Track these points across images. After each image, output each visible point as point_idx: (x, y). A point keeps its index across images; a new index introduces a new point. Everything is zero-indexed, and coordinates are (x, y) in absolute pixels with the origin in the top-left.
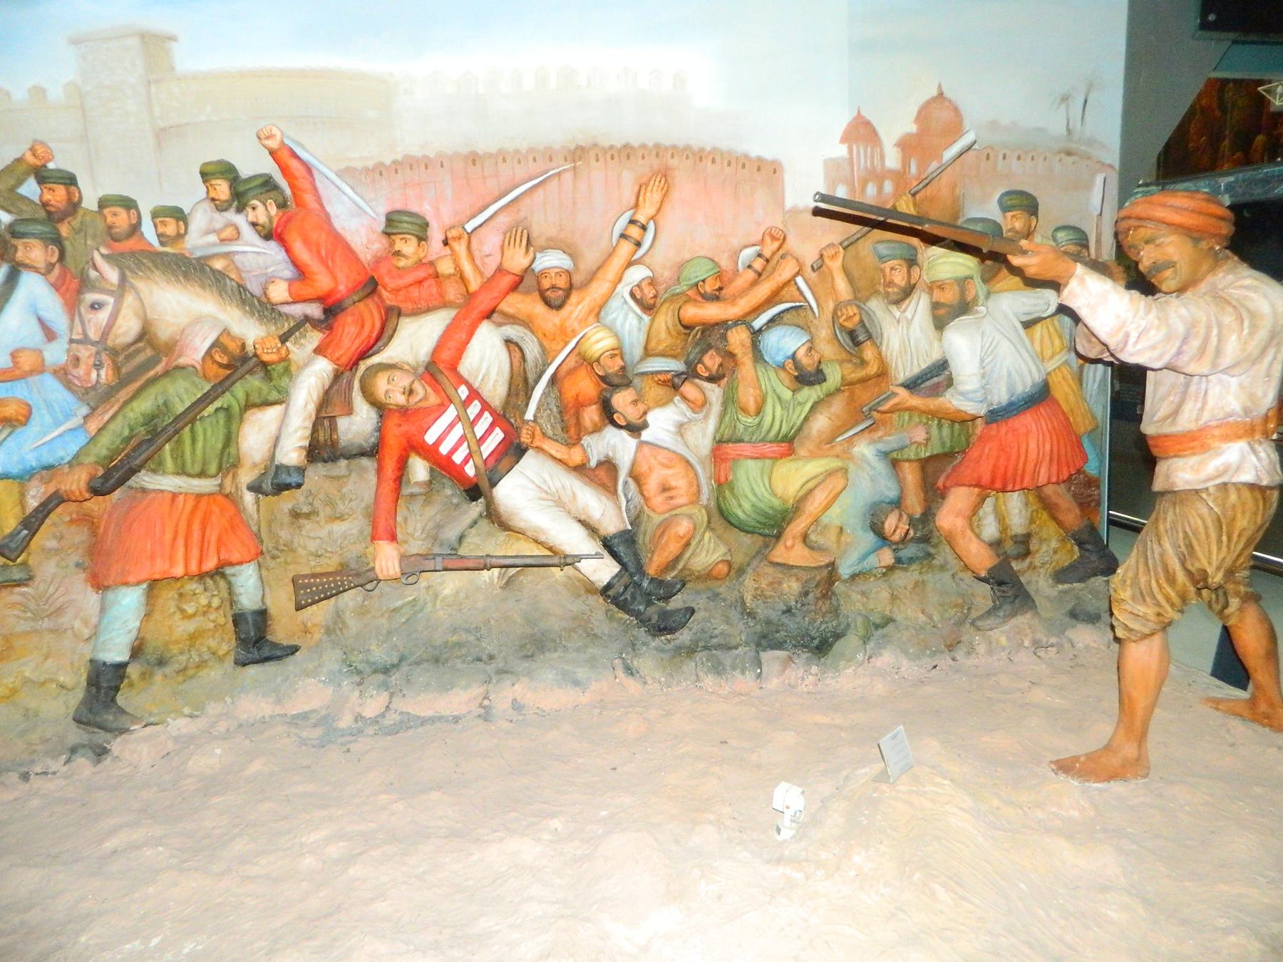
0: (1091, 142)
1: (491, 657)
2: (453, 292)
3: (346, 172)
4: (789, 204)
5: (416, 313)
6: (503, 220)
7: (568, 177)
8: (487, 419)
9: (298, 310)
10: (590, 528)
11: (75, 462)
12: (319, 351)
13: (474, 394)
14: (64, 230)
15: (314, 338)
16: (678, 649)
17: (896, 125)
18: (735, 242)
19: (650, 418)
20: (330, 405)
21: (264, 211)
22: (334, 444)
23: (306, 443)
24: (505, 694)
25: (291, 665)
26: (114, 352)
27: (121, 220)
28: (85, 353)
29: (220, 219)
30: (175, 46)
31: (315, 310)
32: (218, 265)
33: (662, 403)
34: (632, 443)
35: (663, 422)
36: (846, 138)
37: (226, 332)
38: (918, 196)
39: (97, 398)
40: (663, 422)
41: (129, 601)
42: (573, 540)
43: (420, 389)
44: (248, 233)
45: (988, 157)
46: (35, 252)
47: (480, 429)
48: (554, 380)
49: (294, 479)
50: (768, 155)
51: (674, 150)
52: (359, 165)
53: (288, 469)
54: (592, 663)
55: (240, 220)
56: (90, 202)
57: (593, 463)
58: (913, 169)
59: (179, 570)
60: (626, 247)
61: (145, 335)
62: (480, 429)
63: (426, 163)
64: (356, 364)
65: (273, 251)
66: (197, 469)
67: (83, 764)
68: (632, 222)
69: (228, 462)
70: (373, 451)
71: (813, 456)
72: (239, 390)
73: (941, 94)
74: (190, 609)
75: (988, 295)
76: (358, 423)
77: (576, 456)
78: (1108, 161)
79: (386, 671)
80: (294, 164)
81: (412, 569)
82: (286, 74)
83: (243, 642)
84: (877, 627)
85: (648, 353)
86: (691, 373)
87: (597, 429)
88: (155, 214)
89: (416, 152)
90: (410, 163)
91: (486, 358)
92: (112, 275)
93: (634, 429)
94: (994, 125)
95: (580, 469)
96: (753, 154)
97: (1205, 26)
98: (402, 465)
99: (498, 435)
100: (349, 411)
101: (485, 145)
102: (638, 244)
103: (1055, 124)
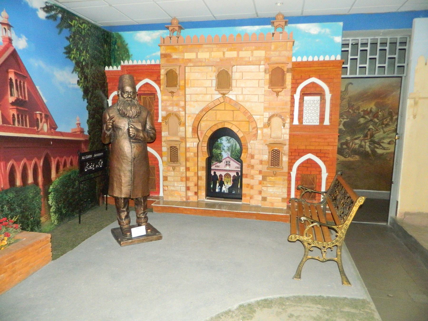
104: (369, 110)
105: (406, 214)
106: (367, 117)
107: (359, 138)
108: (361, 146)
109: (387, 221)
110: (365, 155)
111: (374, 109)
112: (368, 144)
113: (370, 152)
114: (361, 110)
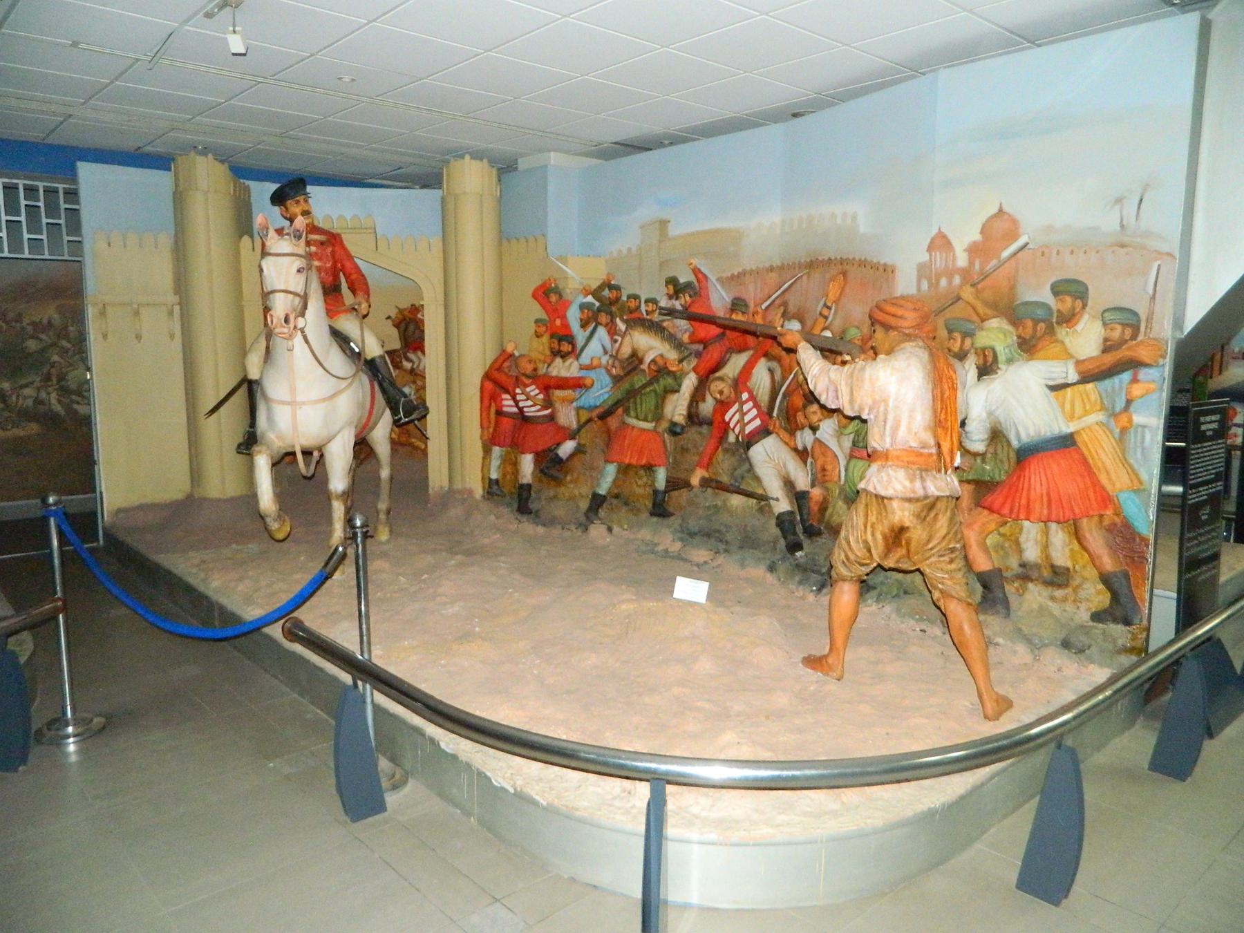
0: (1148, 234)
1: (727, 542)
5: (741, 351)
6: (777, 302)
7: (805, 278)
8: (754, 412)
10: (789, 484)
12: (694, 370)
13: (752, 398)
14: (614, 309)
16: (798, 566)
17: (965, 235)
19: (821, 424)
20: (698, 396)
22: (698, 416)
23: (685, 413)
24: (721, 559)
26: (621, 361)
27: (633, 304)
30: (670, 226)
32: (665, 324)
34: (812, 437)
35: (827, 428)
36: (929, 249)
37: (662, 356)
38: (980, 286)
39: (617, 380)
41: (611, 470)
42: (774, 487)
45: (1043, 254)
46: (604, 318)
47: (747, 418)
49: (678, 430)
50: (890, 262)
52: (724, 275)
53: (674, 424)
54: (759, 559)
56: (624, 298)
57: (800, 447)
58: (977, 267)
59: (634, 462)
60: (821, 320)
62: (747, 418)
64: (707, 377)
66: (642, 416)
67: (579, 533)
68: (825, 305)
69: (658, 416)
70: (710, 423)
72: (662, 382)
73: (1001, 210)
74: (640, 482)
75: (1010, 361)
76: (707, 407)
78: (1165, 248)
79: (692, 535)
80: (700, 276)
81: (705, 483)
83: (654, 505)
84: (906, 593)
87: (803, 429)
88: (646, 301)
90: (743, 274)
91: (761, 378)
93: (814, 429)
94: (1049, 229)
95: (796, 450)
96: (882, 262)
99: (758, 422)
100: (704, 400)
101: (777, 262)
102: (826, 318)
103: (1108, 223)
104: (45, 321)
105: (119, 511)
106: (43, 336)
107: (32, 383)
108: (38, 402)
109: (98, 540)
110: (49, 420)
111: (57, 319)
112: (54, 395)
113: (63, 413)
114: (26, 321)
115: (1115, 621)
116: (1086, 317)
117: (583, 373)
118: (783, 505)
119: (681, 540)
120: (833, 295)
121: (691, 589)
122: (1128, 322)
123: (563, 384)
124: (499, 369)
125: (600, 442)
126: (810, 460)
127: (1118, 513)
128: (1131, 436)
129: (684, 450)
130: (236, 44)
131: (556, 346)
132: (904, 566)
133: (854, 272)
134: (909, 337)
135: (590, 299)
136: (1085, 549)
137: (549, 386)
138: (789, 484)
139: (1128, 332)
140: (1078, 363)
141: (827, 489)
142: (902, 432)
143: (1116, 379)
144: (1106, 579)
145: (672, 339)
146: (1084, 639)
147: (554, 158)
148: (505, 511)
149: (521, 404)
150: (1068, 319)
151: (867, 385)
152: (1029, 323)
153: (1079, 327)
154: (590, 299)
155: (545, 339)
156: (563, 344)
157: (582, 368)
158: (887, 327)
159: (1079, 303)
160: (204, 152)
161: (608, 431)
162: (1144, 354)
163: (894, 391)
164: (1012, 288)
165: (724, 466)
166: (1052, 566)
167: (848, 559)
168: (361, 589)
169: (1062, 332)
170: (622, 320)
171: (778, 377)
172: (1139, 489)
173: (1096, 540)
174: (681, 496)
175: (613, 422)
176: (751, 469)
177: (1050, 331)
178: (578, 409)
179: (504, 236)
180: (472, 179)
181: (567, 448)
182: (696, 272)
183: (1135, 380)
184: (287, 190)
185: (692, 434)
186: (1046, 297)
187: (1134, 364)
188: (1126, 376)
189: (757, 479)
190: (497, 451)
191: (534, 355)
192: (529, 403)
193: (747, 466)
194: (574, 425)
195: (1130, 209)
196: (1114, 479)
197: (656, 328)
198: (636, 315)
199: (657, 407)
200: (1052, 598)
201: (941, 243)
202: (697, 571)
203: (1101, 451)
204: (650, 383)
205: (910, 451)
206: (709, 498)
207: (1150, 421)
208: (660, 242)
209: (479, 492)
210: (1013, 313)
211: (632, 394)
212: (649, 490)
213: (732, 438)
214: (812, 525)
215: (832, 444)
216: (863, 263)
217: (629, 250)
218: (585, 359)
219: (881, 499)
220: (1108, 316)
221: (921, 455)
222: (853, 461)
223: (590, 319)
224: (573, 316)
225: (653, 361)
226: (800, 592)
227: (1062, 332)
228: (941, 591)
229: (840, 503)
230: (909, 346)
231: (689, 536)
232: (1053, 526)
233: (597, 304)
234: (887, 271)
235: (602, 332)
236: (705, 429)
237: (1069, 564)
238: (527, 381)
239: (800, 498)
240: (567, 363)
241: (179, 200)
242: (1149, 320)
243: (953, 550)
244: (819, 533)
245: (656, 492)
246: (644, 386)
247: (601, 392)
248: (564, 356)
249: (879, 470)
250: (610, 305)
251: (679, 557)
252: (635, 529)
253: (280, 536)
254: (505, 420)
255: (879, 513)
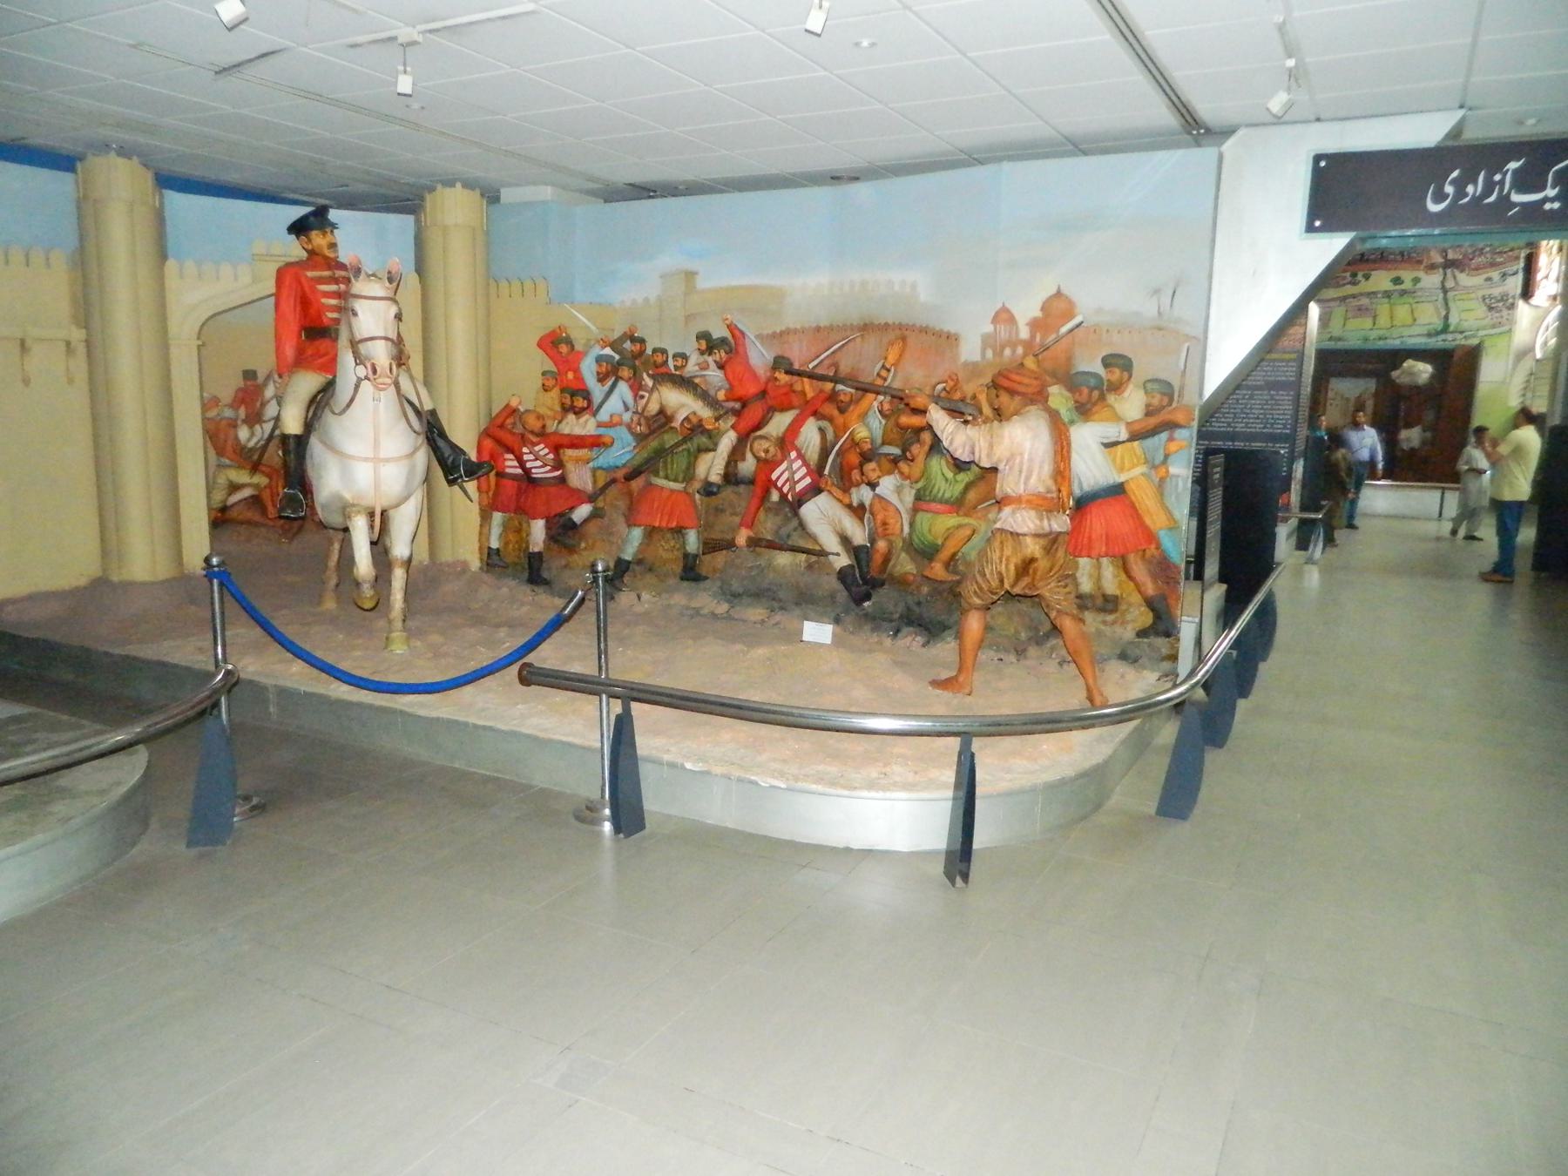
2: (796, 400)
3: (760, 337)
4: (963, 359)
5: (783, 409)
8: (804, 470)
9: (731, 404)
10: (845, 540)
11: (624, 465)
12: (733, 427)
13: (800, 456)
15: (732, 420)
17: (1027, 310)
18: (934, 381)
20: (736, 454)
21: (721, 355)
24: (778, 617)
25: (702, 585)
27: (659, 359)
28: (635, 418)
29: (702, 359)
31: (737, 405)
32: (697, 381)
33: (890, 473)
35: (888, 485)
36: (995, 320)
39: (641, 438)
40: (887, 485)
41: (637, 534)
42: (831, 543)
43: (772, 450)
44: (713, 365)
46: (625, 372)
47: (797, 477)
48: (838, 454)
50: (953, 331)
51: (911, 328)
55: (710, 359)
56: (649, 351)
61: (662, 412)
63: (795, 331)
64: (748, 435)
65: (720, 374)
69: (689, 476)
70: (752, 482)
71: (966, 515)
73: (1059, 294)
75: (1072, 422)
76: (748, 466)
77: (847, 501)
79: (736, 596)
81: (754, 543)
82: (741, 287)
85: (883, 443)
86: (904, 457)
87: (858, 485)
89: (792, 326)
91: (810, 435)
92: (649, 382)
93: (873, 485)
94: (1099, 311)
95: (849, 506)
97: (1310, 228)
98: (767, 492)
99: (808, 480)
100: (744, 459)
103: (1149, 309)
115: (1157, 634)
116: (1131, 386)
117: (601, 431)
118: (843, 561)
119: (728, 601)
120: (891, 358)
121: (818, 632)
122: (1167, 390)
123: (577, 442)
124: (502, 426)
125: (622, 504)
126: (867, 515)
127: (1158, 546)
128: (1168, 485)
129: (719, 511)
130: (405, 84)
131: (568, 401)
132: (1029, 593)
133: (912, 339)
134: (1032, 402)
135: (608, 351)
136: (1131, 578)
137: (559, 445)
138: (845, 540)
139: (1166, 400)
140: (1128, 424)
141: (890, 543)
142: (1033, 480)
143: (1156, 438)
144: (1150, 603)
145: (705, 396)
146: (1138, 652)
147: (547, 192)
148: (513, 583)
149: (529, 465)
150: (1116, 388)
151: (1006, 441)
152: (1086, 391)
153: (1126, 394)
154: (608, 351)
155: (555, 393)
156: (576, 399)
157: (599, 425)
158: (1012, 393)
159: (1126, 375)
160: (124, 152)
161: (630, 494)
162: (1180, 417)
163: (1020, 447)
164: (1069, 359)
165: (768, 526)
166: (1104, 596)
167: (981, 588)
168: (602, 632)
169: (1111, 398)
170: (651, 376)
171: (830, 436)
172: (1173, 526)
173: (1140, 570)
174: (720, 558)
175: (637, 484)
176: (802, 526)
177: (1102, 398)
178: (594, 470)
179: (490, 278)
180: (454, 209)
181: (581, 512)
182: (732, 328)
183: (1171, 439)
184: (312, 219)
185: (728, 493)
186: (1099, 369)
187: (1171, 426)
188: (1164, 436)
189: (813, 538)
190: (498, 517)
191: (542, 410)
192: (539, 463)
193: (795, 523)
194: (589, 487)
195: (1166, 300)
196: (1155, 520)
197: (685, 383)
198: (663, 370)
199: (688, 469)
200: (1104, 623)
201: (1004, 316)
202: (818, 619)
203: (1143, 496)
204: (684, 440)
205: (1039, 495)
206: (747, 560)
207: (1182, 471)
208: (686, 294)
209: (475, 563)
210: (1072, 382)
211: (661, 453)
212: (679, 554)
213: (775, 496)
214: (873, 578)
215: (894, 499)
216: (924, 330)
217: (646, 300)
218: (604, 415)
219: (1015, 535)
220: (1149, 386)
221: (1045, 498)
222: (920, 516)
223: (610, 372)
224: (588, 369)
225: (687, 419)
226: (875, 638)
227: (1111, 398)
228: (1059, 611)
229: (903, 555)
230: (1033, 408)
231: (734, 597)
232: (1105, 561)
233: (617, 357)
234: (951, 339)
235: (623, 389)
236: (742, 488)
237: (1118, 592)
238: (535, 439)
239: (857, 552)
240: (583, 420)
241: (87, 212)
242: (1182, 388)
243: (1068, 576)
244: (883, 584)
245: (686, 555)
246: (677, 445)
247: (622, 451)
248: (578, 412)
249: (1014, 512)
250: (633, 360)
251: (728, 617)
252: (664, 596)
253: (368, 605)
254: (505, 481)
255: (1014, 548)
